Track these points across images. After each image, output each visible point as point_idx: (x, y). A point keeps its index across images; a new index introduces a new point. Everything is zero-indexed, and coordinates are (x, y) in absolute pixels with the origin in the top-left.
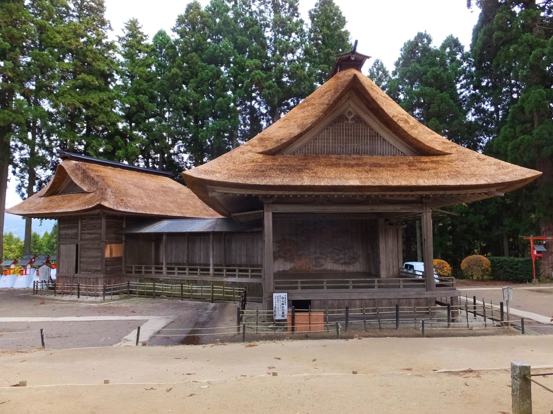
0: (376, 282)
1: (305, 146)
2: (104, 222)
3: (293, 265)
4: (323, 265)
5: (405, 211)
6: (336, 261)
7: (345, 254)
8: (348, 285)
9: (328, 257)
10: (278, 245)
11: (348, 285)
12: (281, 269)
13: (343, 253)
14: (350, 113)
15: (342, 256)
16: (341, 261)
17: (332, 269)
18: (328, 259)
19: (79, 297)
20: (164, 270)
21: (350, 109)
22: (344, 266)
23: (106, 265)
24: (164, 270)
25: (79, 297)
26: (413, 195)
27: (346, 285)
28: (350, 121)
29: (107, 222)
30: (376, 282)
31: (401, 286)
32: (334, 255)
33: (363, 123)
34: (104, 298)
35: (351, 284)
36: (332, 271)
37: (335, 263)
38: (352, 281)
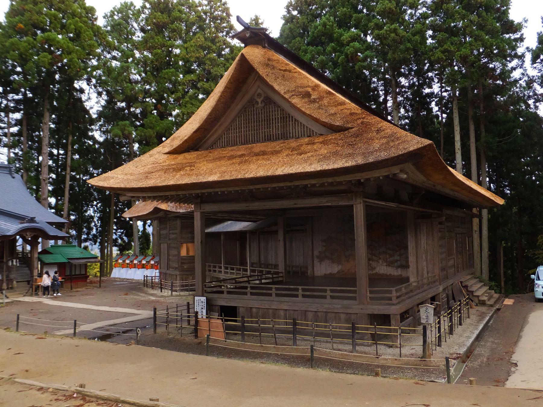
0: (300, 291)
1: (220, 139)
2: (178, 223)
3: (340, 267)
4: (375, 268)
5: (330, 204)
6: (390, 264)
7: (400, 255)
8: (271, 292)
9: (380, 259)
10: (324, 244)
11: (271, 292)
12: (328, 272)
13: (398, 253)
14: (259, 95)
15: (397, 257)
16: (396, 264)
17: (385, 272)
18: (380, 261)
19: (161, 291)
20: (223, 270)
21: (259, 91)
22: (399, 270)
23: (182, 263)
24: (223, 270)
25: (161, 291)
26: (340, 183)
27: (269, 292)
28: (260, 105)
29: (182, 223)
30: (300, 291)
31: (328, 297)
32: (388, 256)
33: (273, 104)
34: (172, 293)
35: (273, 291)
36: (386, 275)
37: (389, 266)
38: (275, 288)
